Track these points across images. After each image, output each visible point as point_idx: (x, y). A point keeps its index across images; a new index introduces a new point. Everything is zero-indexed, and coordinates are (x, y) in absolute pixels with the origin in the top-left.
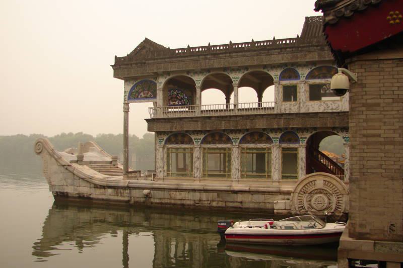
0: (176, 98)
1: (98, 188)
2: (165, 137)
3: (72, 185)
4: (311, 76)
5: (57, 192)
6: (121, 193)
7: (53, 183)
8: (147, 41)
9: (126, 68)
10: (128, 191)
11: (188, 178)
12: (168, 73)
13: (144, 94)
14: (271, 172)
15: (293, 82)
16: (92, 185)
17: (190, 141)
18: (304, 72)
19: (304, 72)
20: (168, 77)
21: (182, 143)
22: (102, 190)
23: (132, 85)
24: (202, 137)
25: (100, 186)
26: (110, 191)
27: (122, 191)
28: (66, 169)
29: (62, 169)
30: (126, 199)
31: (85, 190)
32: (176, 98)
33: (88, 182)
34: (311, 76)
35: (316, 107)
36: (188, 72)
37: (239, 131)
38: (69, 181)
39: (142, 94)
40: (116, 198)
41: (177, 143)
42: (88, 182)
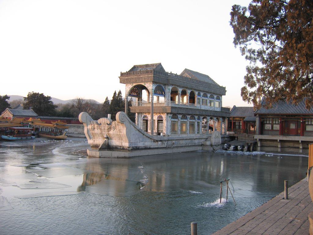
0: (135, 91)
1: (154, 142)
2: (171, 115)
3: (142, 141)
4: (203, 96)
5: (133, 147)
6: (164, 144)
7: (131, 142)
8: (160, 64)
9: (158, 77)
10: (166, 142)
11: (176, 134)
12: (172, 85)
13: (159, 92)
14: (195, 131)
15: (200, 97)
16: (153, 140)
17: (177, 118)
18: (202, 94)
19: (202, 94)
20: (172, 87)
21: (175, 119)
22: (157, 143)
23: (155, 87)
24: (181, 116)
25: (156, 140)
26: (160, 143)
27: (164, 142)
28: (141, 132)
29: (137, 132)
30: (166, 146)
31: (148, 143)
32: (135, 91)
33: (151, 139)
34: (203, 96)
35: (203, 107)
36: (178, 86)
37: (189, 114)
38: (141, 139)
39: (158, 92)
40: (162, 146)
41: (174, 119)
42: (151, 139)
